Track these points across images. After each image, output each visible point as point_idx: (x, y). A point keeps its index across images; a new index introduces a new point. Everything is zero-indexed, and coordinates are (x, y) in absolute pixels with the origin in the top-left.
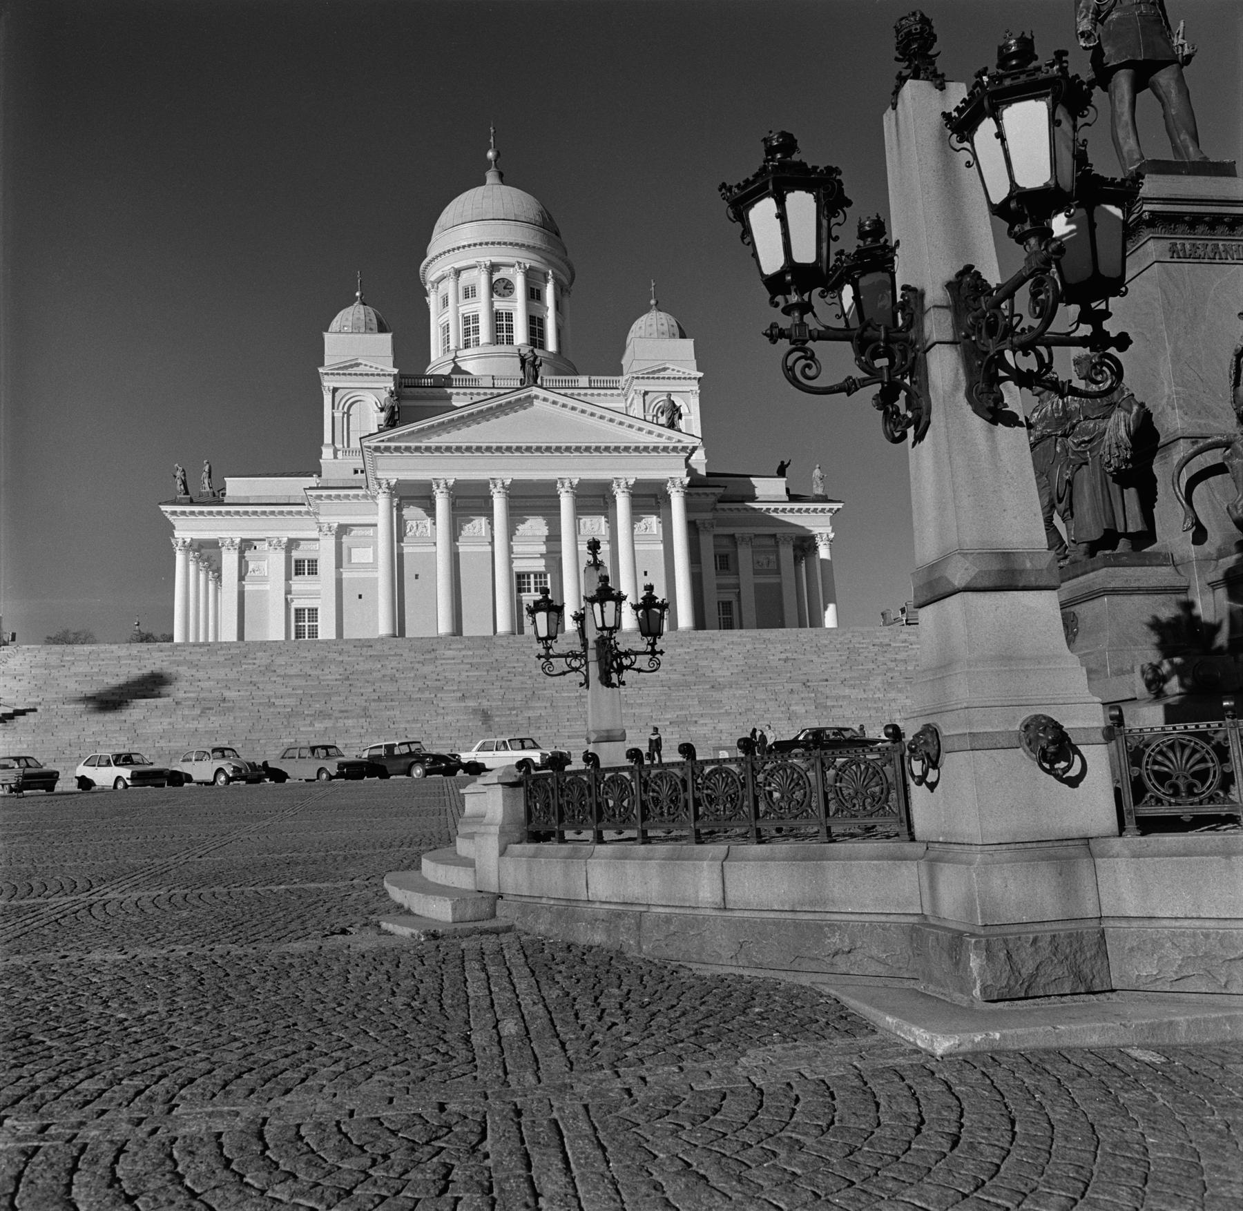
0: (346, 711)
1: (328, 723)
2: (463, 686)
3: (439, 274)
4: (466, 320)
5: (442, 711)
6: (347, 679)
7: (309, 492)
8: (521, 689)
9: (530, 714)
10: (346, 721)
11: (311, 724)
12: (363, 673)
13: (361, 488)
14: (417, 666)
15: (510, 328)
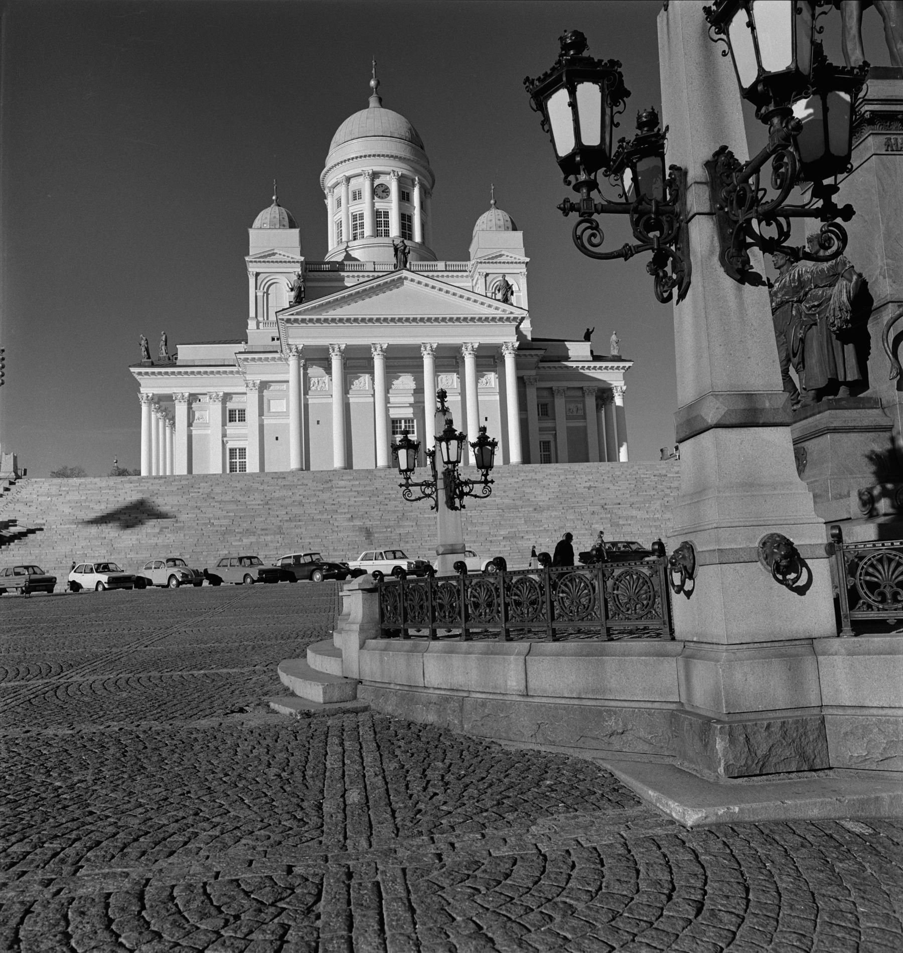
0: (266, 530)
1: (253, 539)
2: (352, 509)
3: (334, 181)
4: (355, 218)
5: (336, 529)
6: (267, 504)
7: (239, 356)
8: (395, 512)
9: (401, 531)
10: (266, 537)
11: (241, 540)
12: (278, 499)
13: (276, 352)
14: (318, 493)
15: (387, 224)
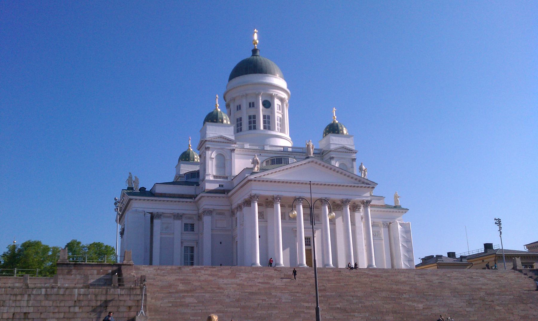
4: (250, 117)
